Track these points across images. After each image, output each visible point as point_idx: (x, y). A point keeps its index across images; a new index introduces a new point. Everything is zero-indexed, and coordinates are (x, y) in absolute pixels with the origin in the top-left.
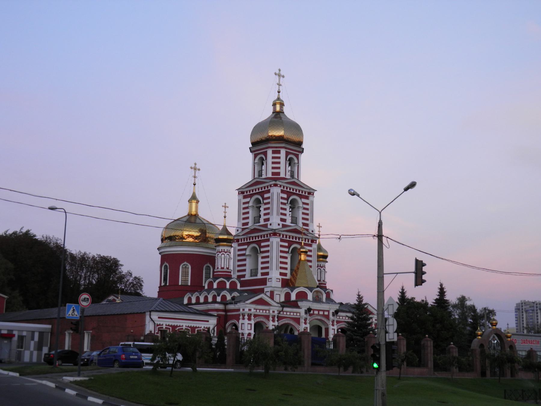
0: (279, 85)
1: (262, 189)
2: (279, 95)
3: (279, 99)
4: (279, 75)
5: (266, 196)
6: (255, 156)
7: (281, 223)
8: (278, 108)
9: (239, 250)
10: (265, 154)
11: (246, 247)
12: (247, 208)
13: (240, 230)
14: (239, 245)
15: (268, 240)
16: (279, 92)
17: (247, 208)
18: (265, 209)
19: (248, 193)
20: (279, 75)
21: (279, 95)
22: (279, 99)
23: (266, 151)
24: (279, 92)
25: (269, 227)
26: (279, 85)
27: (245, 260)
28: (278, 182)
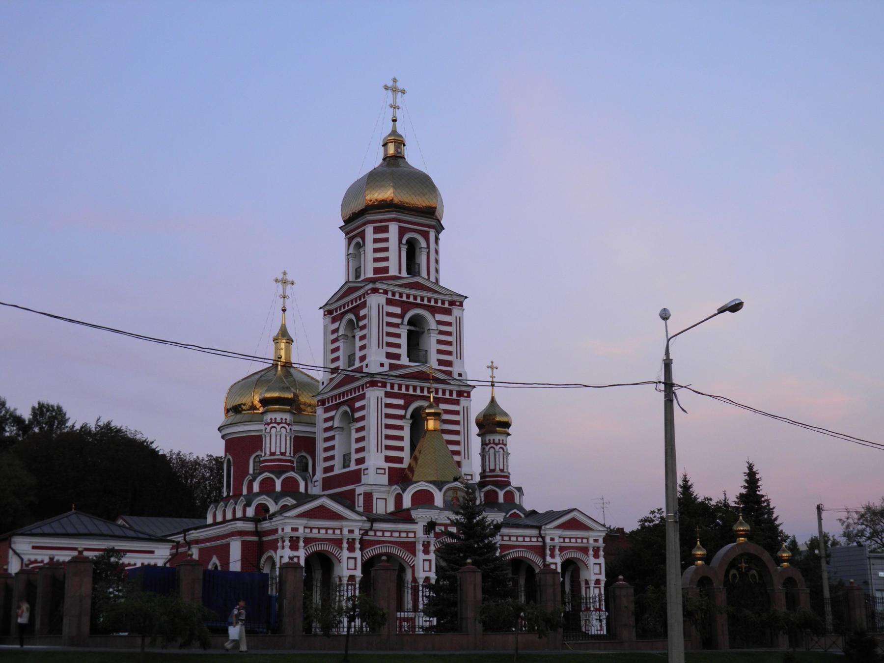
0: (395, 107)
1: (429, 300)
2: (394, 126)
3: (394, 132)
4: (394, 89)
5: (439, 317)
6: (402, 232)
7: (387, 362)
8: (391, 150)
9: (387, 406)
10: (426, 236)
11: (401, 402)
12: (397, 326)
13: (386, 368)
14: (388, 395)
15: (457, 402)
16: (394, 121)
17: (397, 326)
18: (439, 342)
19: (397, 297)
20: (394, 89)
21: (394, 126)
22: (394, 132)
23: (428, 232)
24: (394, 121)
25: (456, 376)
26: (395, 107)
27: (401, 428)
28: (378, 285)
